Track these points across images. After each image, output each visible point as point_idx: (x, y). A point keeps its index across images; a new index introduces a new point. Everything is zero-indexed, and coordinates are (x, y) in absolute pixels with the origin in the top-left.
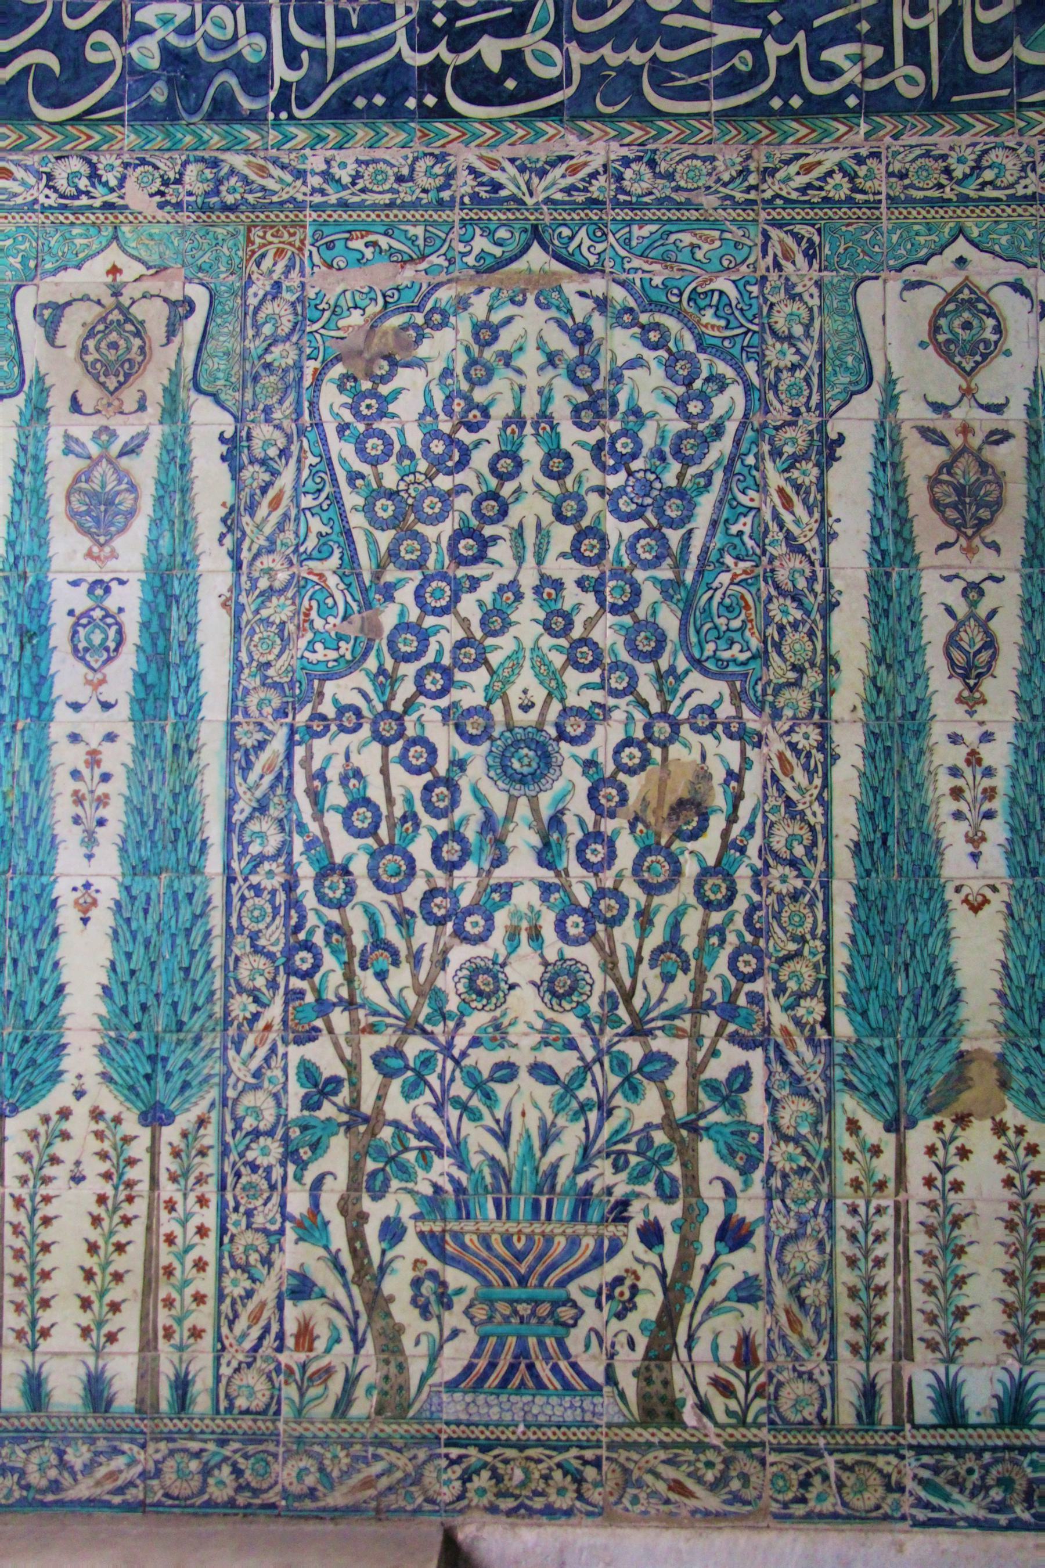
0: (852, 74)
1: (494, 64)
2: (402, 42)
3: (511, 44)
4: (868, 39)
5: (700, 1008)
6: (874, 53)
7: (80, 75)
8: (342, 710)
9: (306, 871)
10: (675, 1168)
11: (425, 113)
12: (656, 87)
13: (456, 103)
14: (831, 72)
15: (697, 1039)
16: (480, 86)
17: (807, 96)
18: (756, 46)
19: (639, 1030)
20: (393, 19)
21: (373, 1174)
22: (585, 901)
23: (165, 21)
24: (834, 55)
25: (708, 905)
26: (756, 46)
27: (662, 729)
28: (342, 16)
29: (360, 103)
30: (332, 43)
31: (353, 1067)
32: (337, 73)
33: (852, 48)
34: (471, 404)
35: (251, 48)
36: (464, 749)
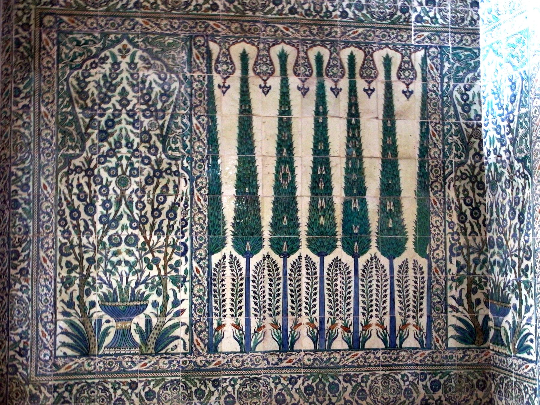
5: (167, 246)
8: (77, 167)
9: (67, 212)
10: (161, 287)
15: (166, 254)
19: (151, 251)
21: (87, 290)
22: (137, 219)
25: (170, 219)
27: (158, 174)
31: (81, 262)
34: (111, 85)
36: (110, 179)
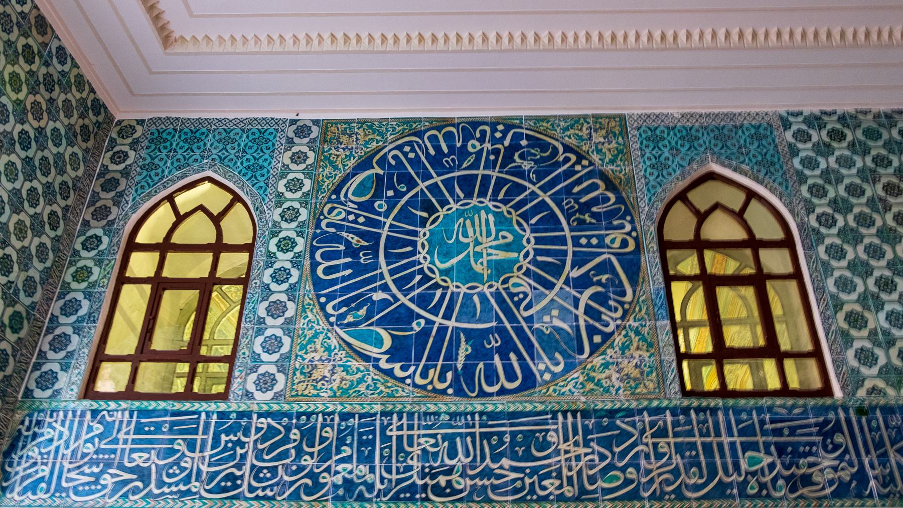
0: (551, 489)
1: (443, 484)
2: (415, 477)
3: (449, 478)
4: (556, 477)
6: (557, 483)
7: (318, 486)
11: (423, 500)
12: (492, 491)
13: (432, 497)
14: (544, 488)
16: (438, 491)
17: (538, 496)
18: (522, 479)
20: (412, 470)
23: (345, 470)
24: (546, 483)
26: (522, 479)
28: (398, 468)
29: (402, 496)
30: (394, 477)
32: (396, 486)
33: (550, 481)
35: (369, 478)
